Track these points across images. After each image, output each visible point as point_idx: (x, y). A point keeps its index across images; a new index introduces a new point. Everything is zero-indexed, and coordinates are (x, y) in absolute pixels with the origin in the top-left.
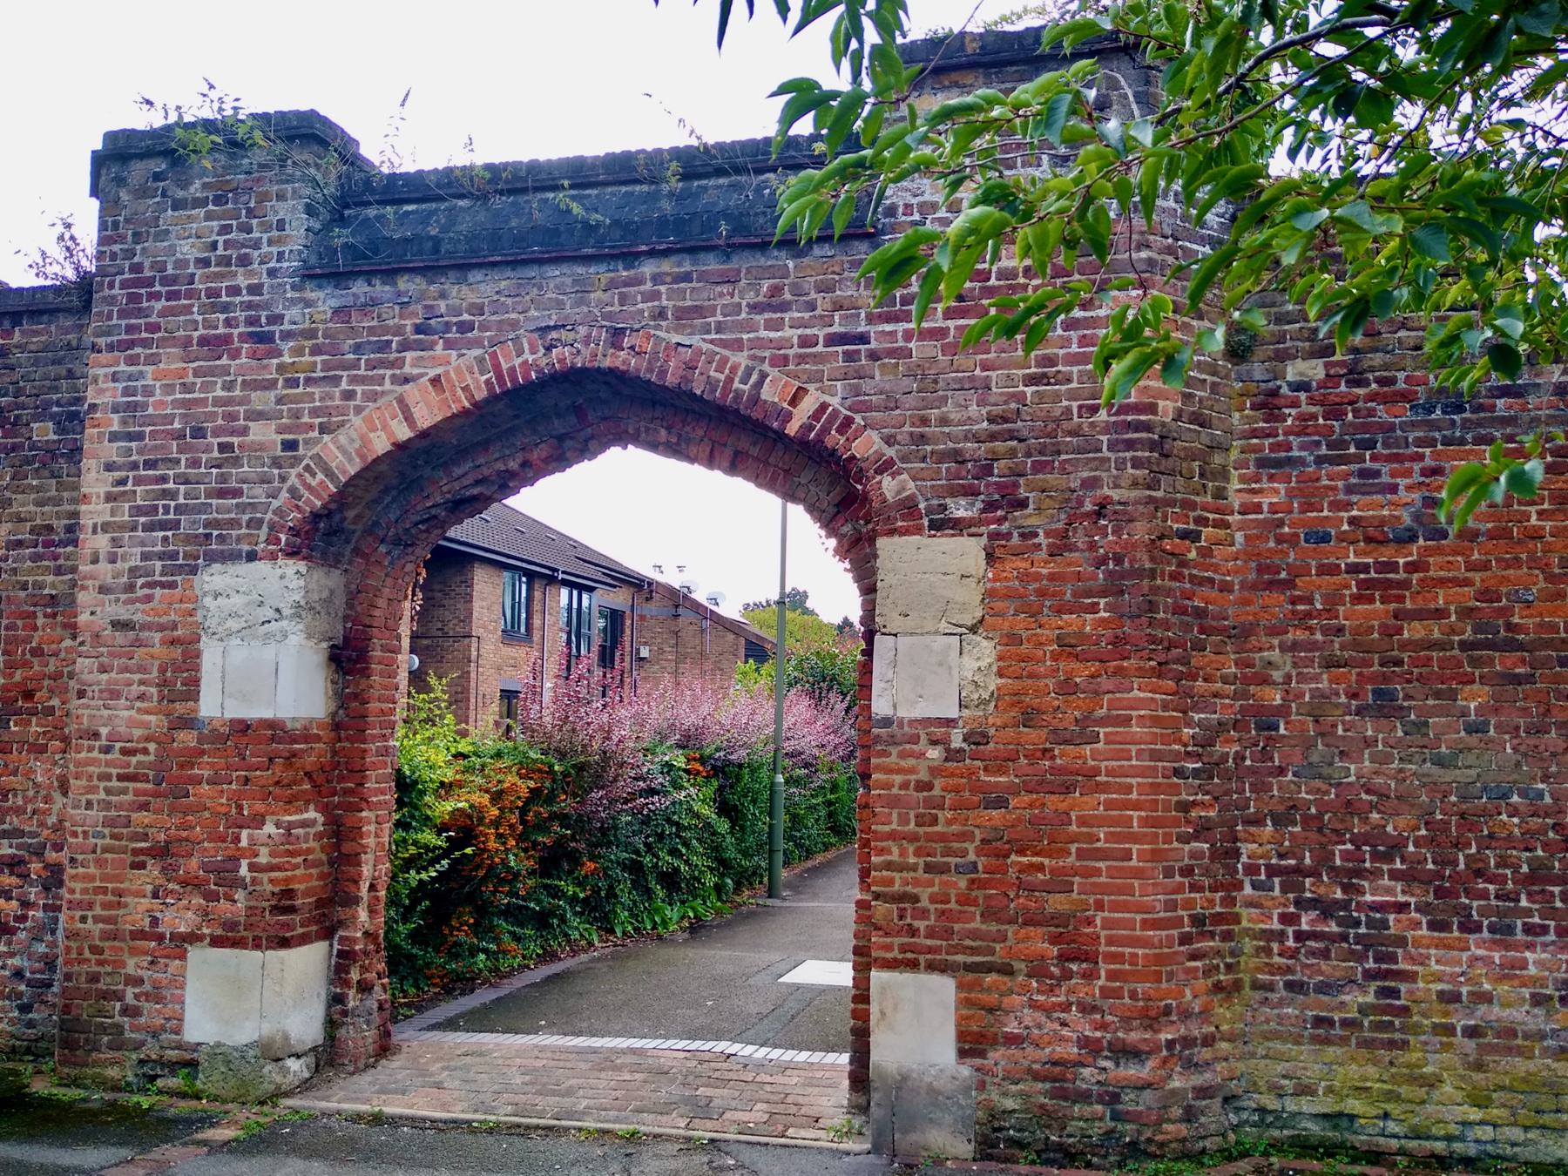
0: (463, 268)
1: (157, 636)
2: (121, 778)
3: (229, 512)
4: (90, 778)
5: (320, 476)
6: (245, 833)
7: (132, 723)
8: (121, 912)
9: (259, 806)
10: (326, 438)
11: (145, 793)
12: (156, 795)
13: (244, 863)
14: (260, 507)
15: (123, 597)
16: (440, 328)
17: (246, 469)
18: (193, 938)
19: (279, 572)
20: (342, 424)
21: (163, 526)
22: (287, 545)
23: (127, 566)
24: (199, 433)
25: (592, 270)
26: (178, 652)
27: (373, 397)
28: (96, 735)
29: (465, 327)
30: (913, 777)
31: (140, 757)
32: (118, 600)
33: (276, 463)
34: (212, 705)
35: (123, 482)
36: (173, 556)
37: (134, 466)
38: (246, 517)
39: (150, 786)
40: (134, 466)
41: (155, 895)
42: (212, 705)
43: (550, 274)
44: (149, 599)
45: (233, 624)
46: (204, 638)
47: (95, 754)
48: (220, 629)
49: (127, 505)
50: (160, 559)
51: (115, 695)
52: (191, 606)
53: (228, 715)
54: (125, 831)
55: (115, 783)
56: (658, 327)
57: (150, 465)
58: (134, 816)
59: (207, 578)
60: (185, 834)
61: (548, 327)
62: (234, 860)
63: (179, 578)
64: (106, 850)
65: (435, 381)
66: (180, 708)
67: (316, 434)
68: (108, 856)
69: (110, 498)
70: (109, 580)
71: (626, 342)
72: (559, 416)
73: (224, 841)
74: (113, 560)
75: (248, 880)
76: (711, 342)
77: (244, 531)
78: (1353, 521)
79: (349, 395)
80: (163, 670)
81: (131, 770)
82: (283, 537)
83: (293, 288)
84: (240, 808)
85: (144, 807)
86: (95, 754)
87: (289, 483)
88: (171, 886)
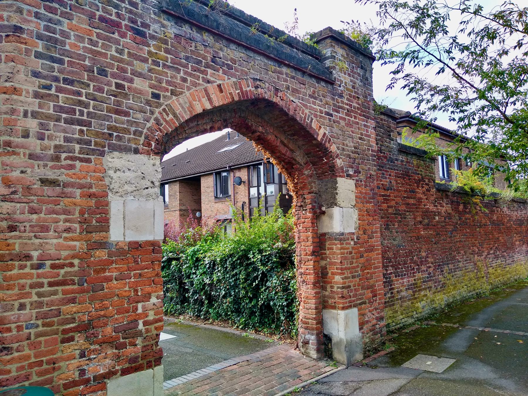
0: (230, 41)
1: (78, 192)
2: (51, 284)
3: (123, 124)
4: (23, 287)
5: (171, 116)
6: (140, 305)
7: (59, 247)
8: (56, 374)
9: (148, 289)
10: (174, 98)
11: (73, 292)
12: (83, 291)
13: (141, 322)
14: (140, 125)
15: (50, 164)
16: (221, 63)
17: (131, 101)
18: (110, 374)
19: (152, 162)
20: (181, 93)
21: (80, 123)
22: (155, 148)
23: (53, 143)
24: (102, 72)
25: (269, 63)
26: (93, 202)
27: (195, 85)
28: (28, 257)
29: (230, 67)
30: (349, 250)
31: (67, 269)
32: (45, 166)
33: (148, 103)
34: (117, 234)
35: (49, 87)
36: (89, 143)
37: (56, 79)
38: (133, 129)
39: (76, 287)
40: (56, 79)
41: (82, 355)
42: (117, 234)
43: (257, 58)
44: (72, 167)
45: (128, 188)
46: (110, 194)
47: (27, 270)
48: (120, 190)
49: (52, 104)
50: (78, 143)
51: (45, 229)
52: (101, 175)
53: (128, 239)
54: (55, 319)
55: (46, 288)
56: (287, 92)
57: (71, 82)
58: (63, 308)
59: (110, 160)
60: (102, 313)
61: (257, 79)
62: (135, 322)
63: (92, 157)
64: (38, 335)
65: (219, 86)
66: (96, 237)
67: (169, 94)
68: (42, 339)
69: (36, 95)
70: (38, 151)
71: (280, 94)
72: (229, 112)
73: (128, 312)
74: (41, 137)
75: (143, 331)
76: (301, 103)
77: (132, 136)
78: (382, 184)
79: (184, 80)
80: (82, 213)
81: (60, 278)
82: (153, 144)
83: (155, 14)
84: (136, 291)
85: (73, 301)
86: (27, 270)
87: (155, 116)
88: (92, 347)
